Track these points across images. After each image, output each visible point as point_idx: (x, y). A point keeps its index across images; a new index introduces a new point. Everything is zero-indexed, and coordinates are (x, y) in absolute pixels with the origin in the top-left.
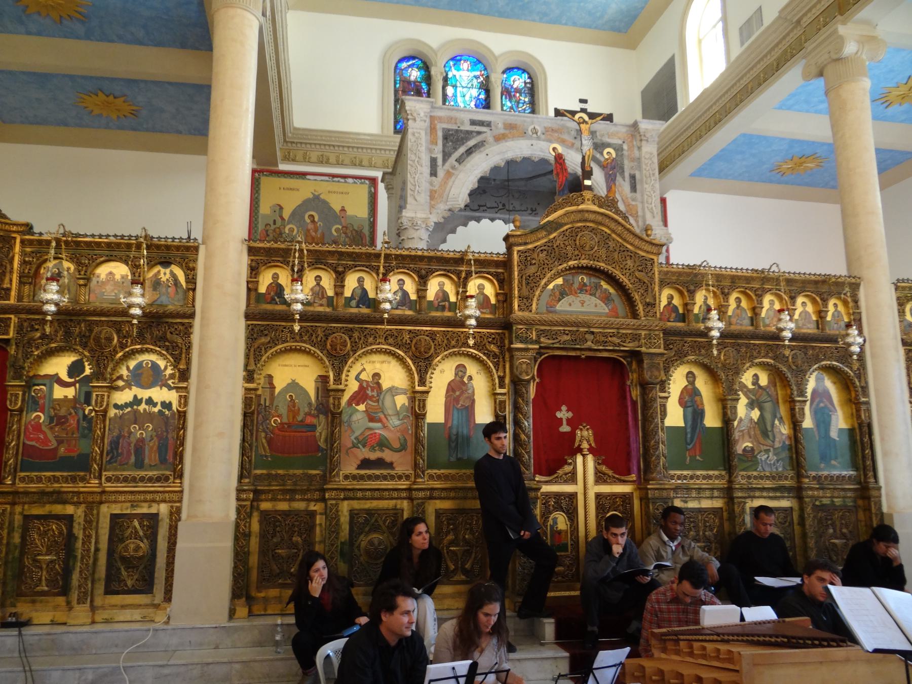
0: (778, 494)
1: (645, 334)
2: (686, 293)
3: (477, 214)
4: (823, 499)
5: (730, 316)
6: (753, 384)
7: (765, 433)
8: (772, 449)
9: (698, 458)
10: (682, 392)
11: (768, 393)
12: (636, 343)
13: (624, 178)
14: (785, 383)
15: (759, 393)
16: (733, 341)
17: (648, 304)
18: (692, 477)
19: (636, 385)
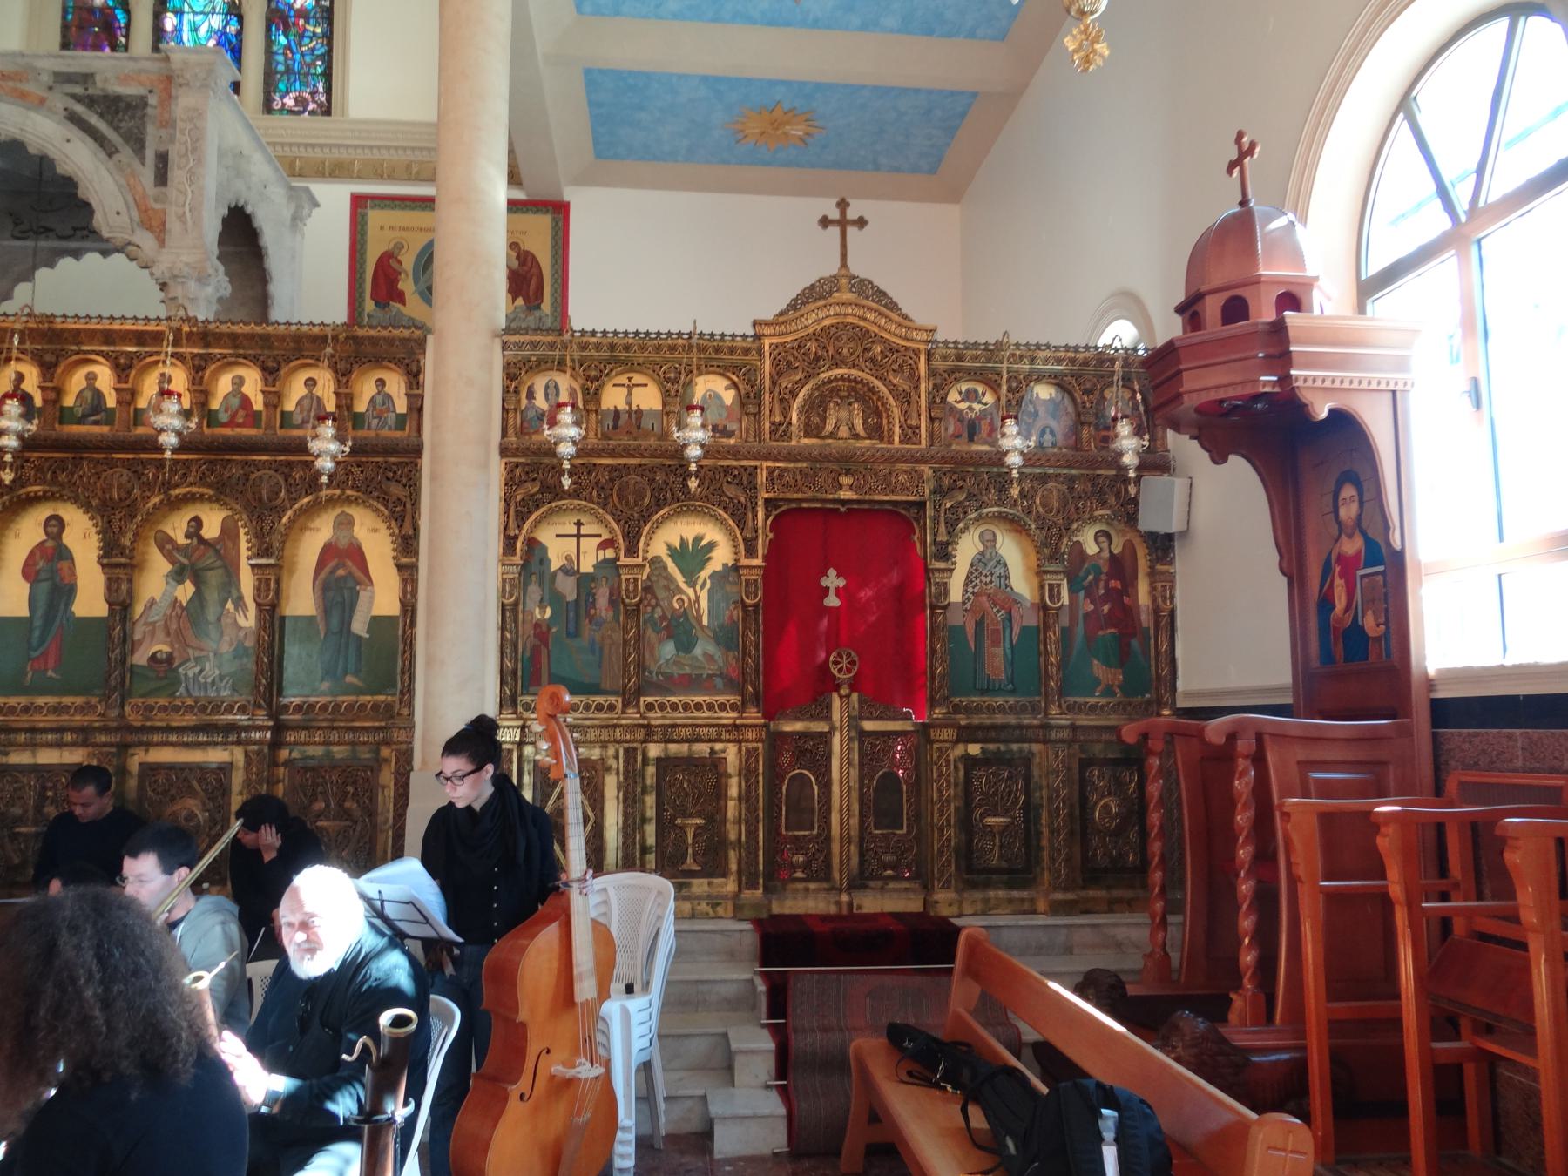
0: (203, 738)
3: (73, 245)
4: (306, 748)
6: (187, 536)
9: (50, 673)
10: (32, 554)
11: (217, 552)
13: (142, 160)
15: (197, 554)
16: (130, 456)
18: (26, 709)
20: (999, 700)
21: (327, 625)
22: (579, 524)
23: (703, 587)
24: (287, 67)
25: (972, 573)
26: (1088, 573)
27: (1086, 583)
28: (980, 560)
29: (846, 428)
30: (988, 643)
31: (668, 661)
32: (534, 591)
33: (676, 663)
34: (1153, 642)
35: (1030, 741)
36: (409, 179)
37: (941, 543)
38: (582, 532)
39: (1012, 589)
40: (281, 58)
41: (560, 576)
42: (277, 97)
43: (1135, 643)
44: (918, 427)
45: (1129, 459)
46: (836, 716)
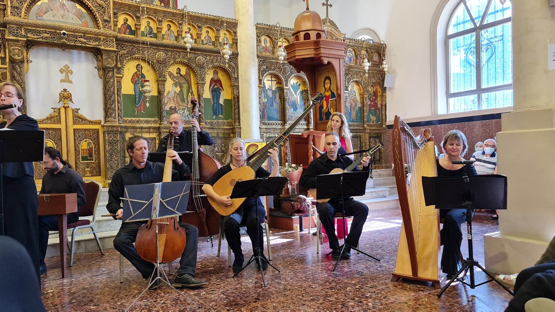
1: (103, 39)
2: (135, 18)
5: (163, 35)
6: (177, 73)
7: (183, 100)
8: (186, 108)
9: (142, 111)
11: (185, 79)
12: (97, 43)
14: (195, 75)
17: (106, 21)
18: (138, 122)
19: (101, 69)
21: (214, 101)
22: (271, 77)
23: (298, 95)
32: (263, 95)
41: (268, 90)
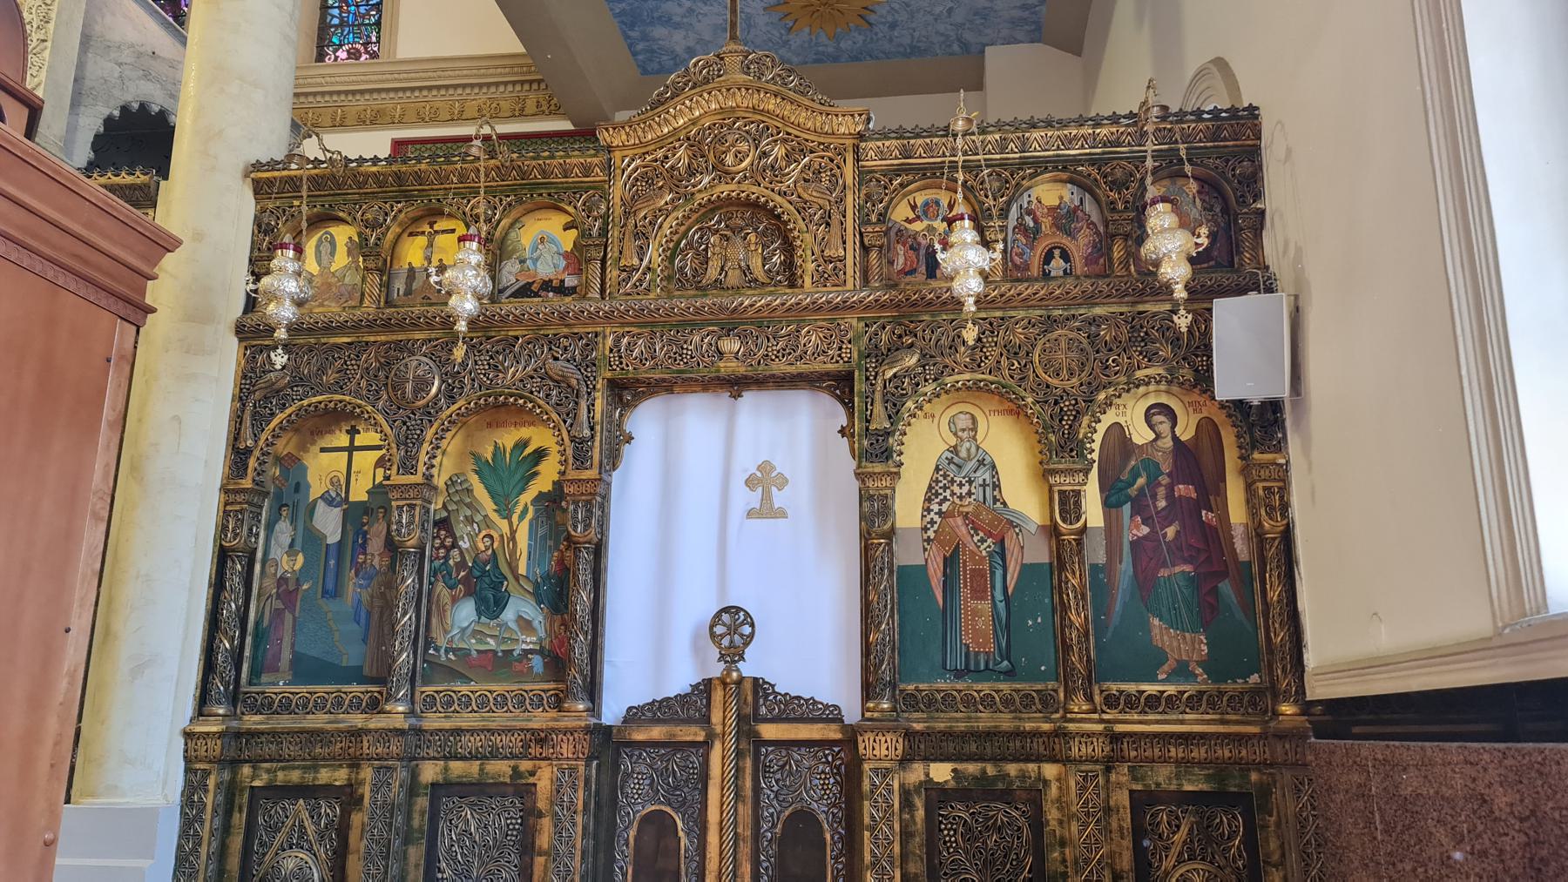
20: (986, 687)
24: (341, 18)
25: (937, 481)
26: (1135, 475)
27: (1133, 491)
28: (950, 461)
29: (738, 272)
30: (965, 592)
31: (463, 630)
33: (475, 633)
34: (1257, 585)
35: (1039, 759)
36: (453, 120)
37: (877, 433)
38: (357, 444)
39: (1004, 504)
40: (336, 12)
41: (321, 506)
42: (330, 51)
43: (1226, 587)
44: (842, 260)
45: (1176, 272)
46: (716, 717)
